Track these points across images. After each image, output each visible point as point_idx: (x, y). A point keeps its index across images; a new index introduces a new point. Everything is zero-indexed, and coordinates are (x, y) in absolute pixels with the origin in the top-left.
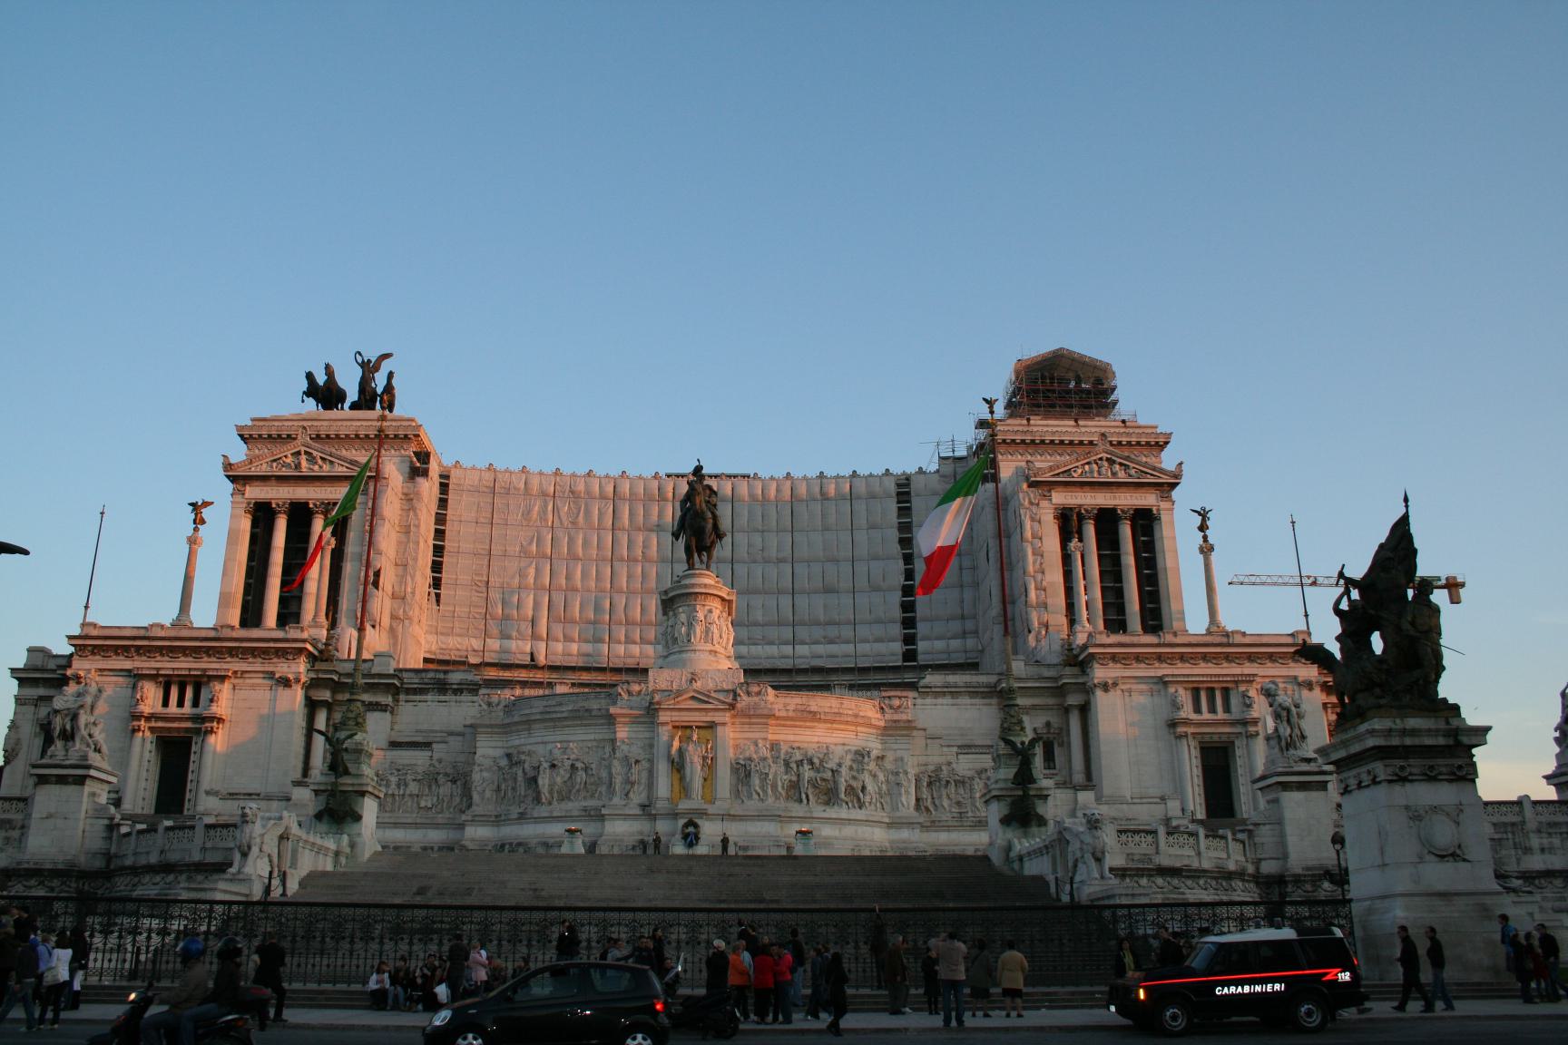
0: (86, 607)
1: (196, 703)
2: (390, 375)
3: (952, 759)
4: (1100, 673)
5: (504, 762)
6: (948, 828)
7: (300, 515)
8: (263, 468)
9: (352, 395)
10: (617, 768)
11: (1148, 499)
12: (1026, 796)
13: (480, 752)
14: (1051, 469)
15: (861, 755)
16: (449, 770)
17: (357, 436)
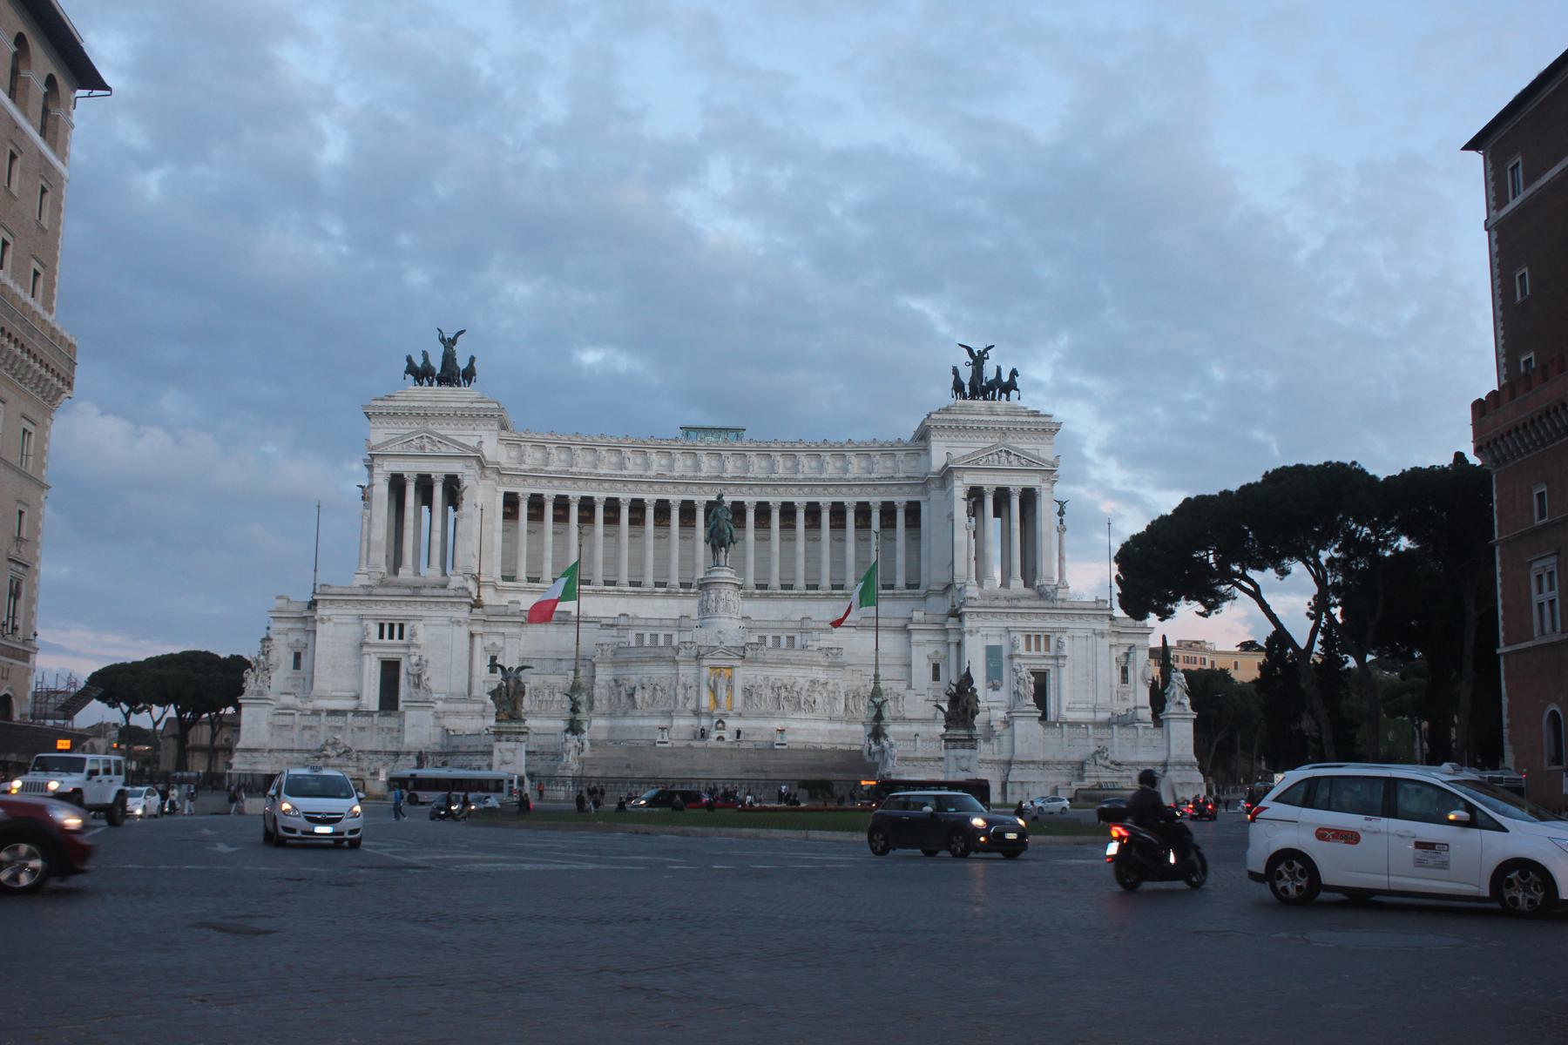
1: (401, 637)
2: (472, 359)
7: (425, 485)
8: (397, 448)
9: (438, 371)
10: (680, 691)
15: (813, 682)
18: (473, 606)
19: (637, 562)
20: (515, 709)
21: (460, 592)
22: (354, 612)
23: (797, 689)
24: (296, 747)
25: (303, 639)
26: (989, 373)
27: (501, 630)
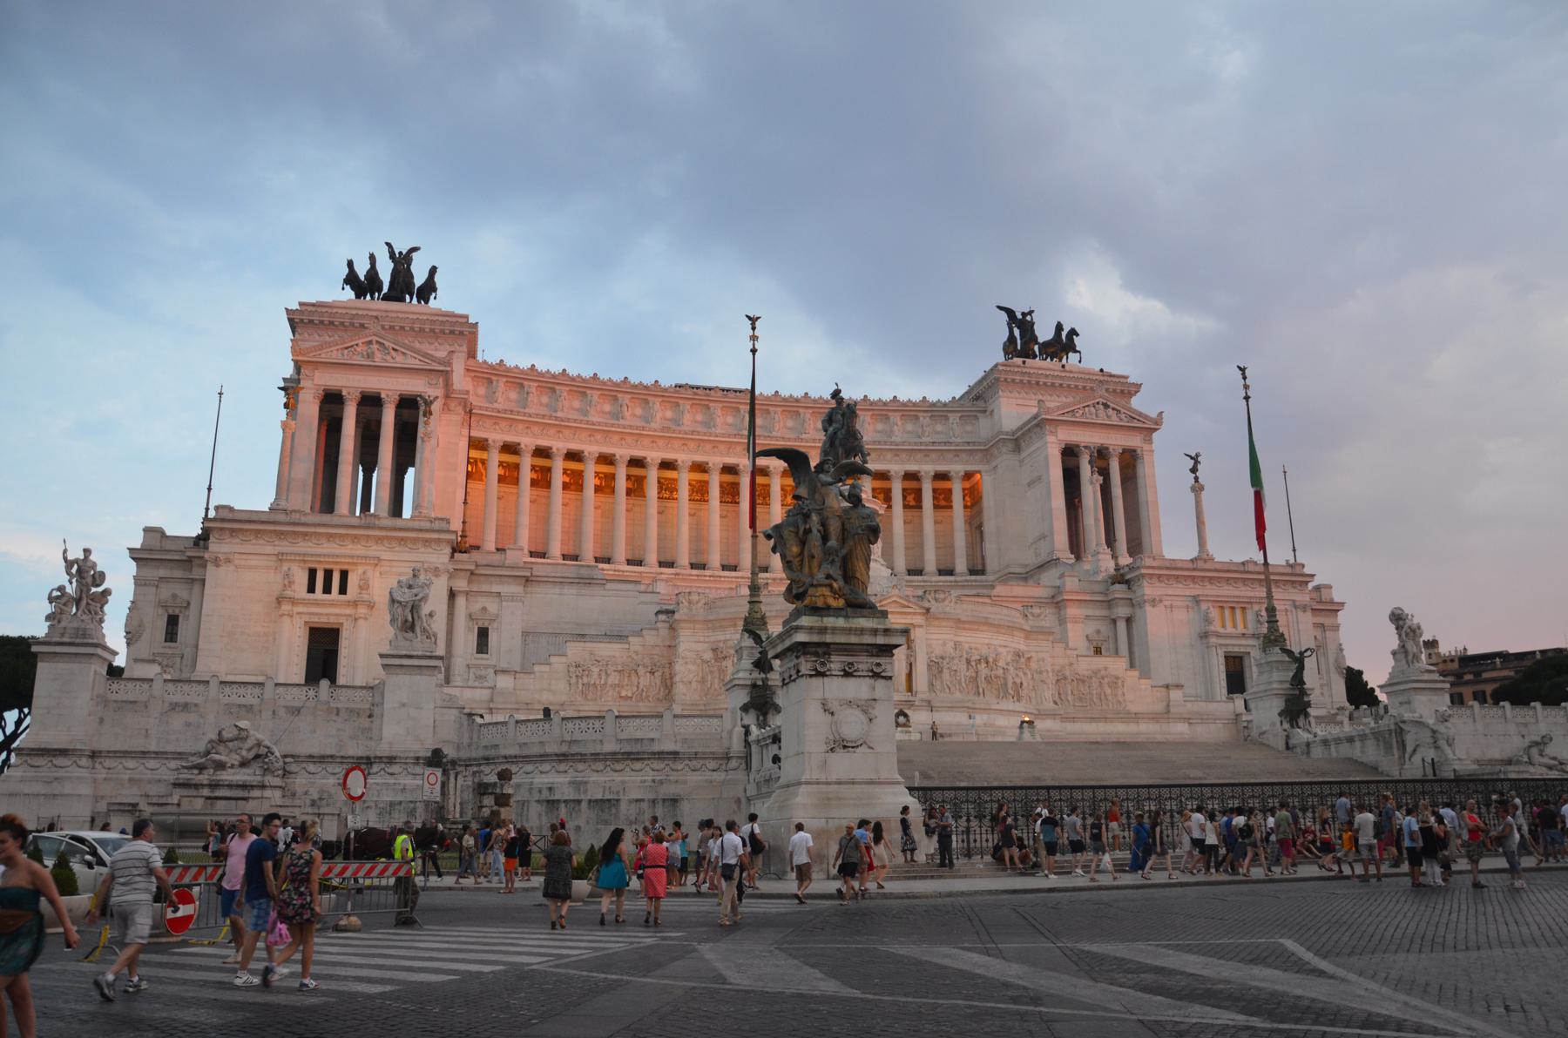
0: (209, 489)
1: (343, 590)
2: (433, 270)
3: (1073, 660)
4: (1148, 590)
5: (708, 655)
6: (1073, 719)
7: (371, 402)
8: (334, 355)
9: (385, 289)
11: (1134, 441)
12: (1303, 693)
13: (682, 648)
14: (1058, 408)
15: (1018, 655)
16: (647, 661)
17: (412, 329)
18: (454, 551)
19: (636, 540)
20: (849, 576)
21: (437, 525)
22: (269, 549)
23: (1001, 664)
24: (153, 748)
25: (182, 592)
26: (1044, 333)
27: (495, 588)
